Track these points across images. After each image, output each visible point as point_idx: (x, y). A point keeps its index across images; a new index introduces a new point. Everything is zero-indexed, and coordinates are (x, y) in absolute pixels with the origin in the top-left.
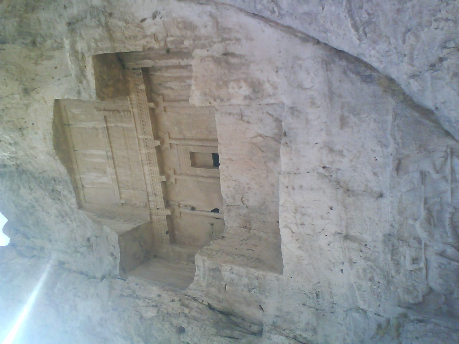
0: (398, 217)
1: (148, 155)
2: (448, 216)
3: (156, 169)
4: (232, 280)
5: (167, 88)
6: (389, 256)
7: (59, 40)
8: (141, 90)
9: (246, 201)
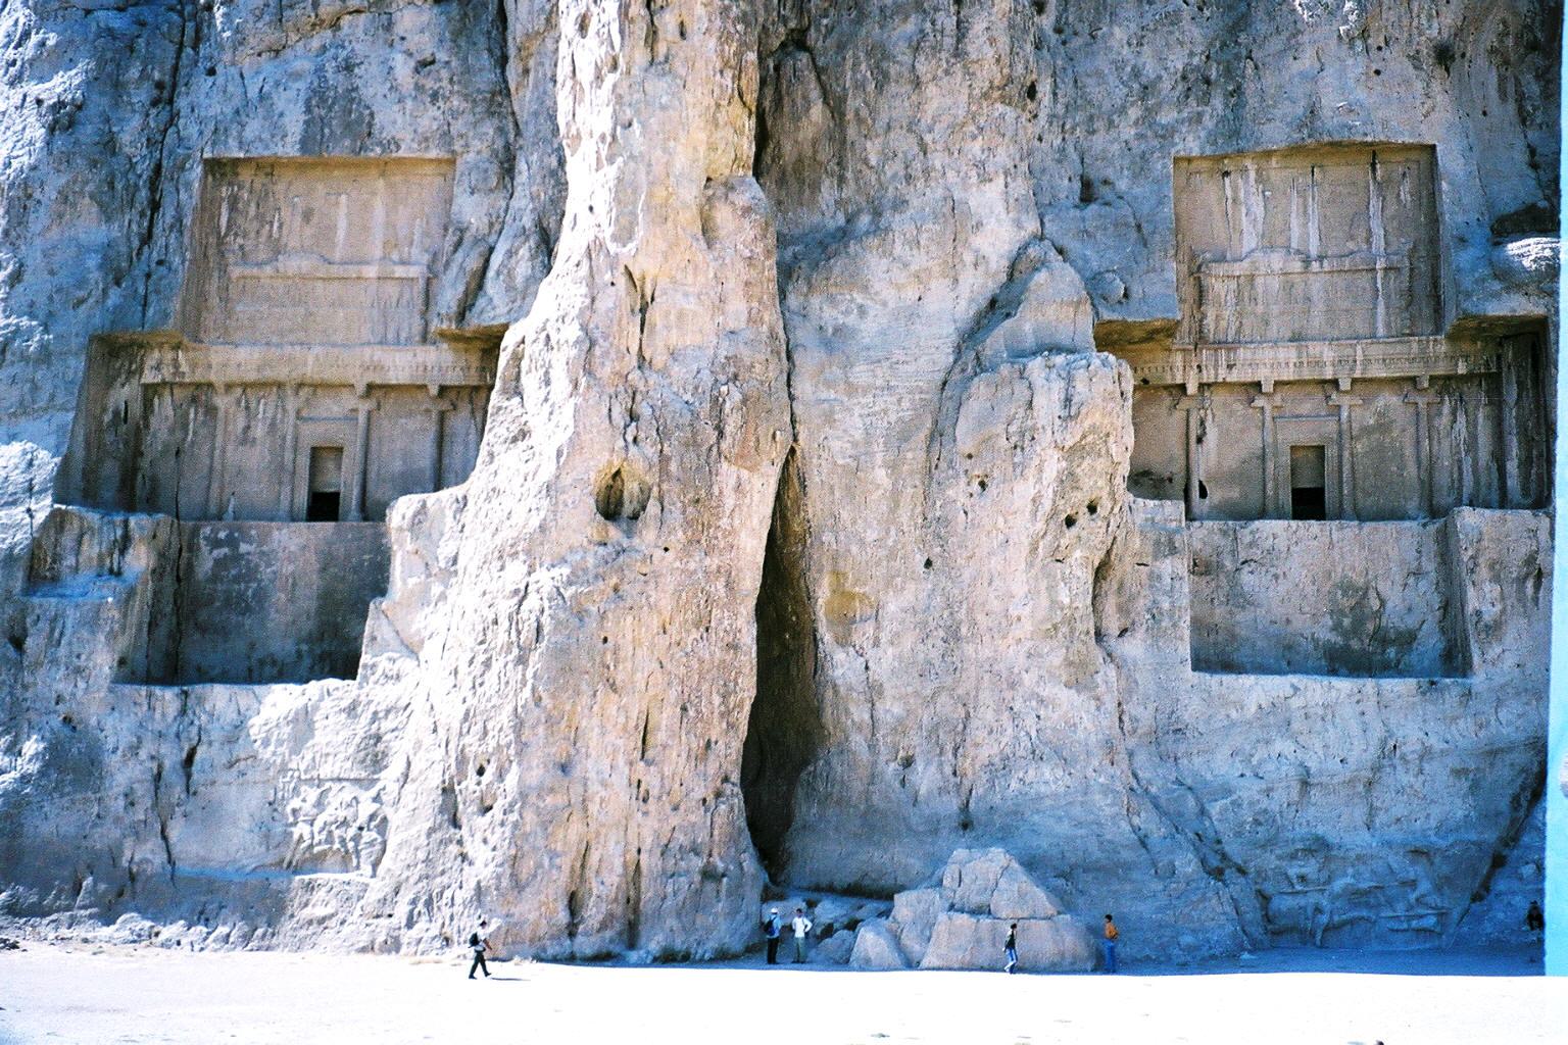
0: (1352, 854)
2: (1365, 913)
4: (1159, 577)
5: (1454, 413)
6: (1300, 846)
8: (1456, 365)
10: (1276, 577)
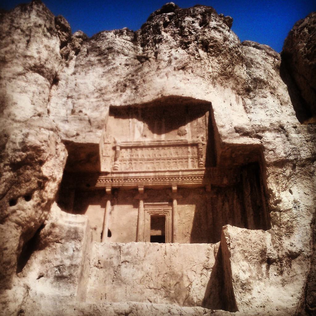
1: (164, 178)
3: (150, 183)
5: (223, 201)
7: (252, 110)
9: (125, 266)
10: (138, 269)
